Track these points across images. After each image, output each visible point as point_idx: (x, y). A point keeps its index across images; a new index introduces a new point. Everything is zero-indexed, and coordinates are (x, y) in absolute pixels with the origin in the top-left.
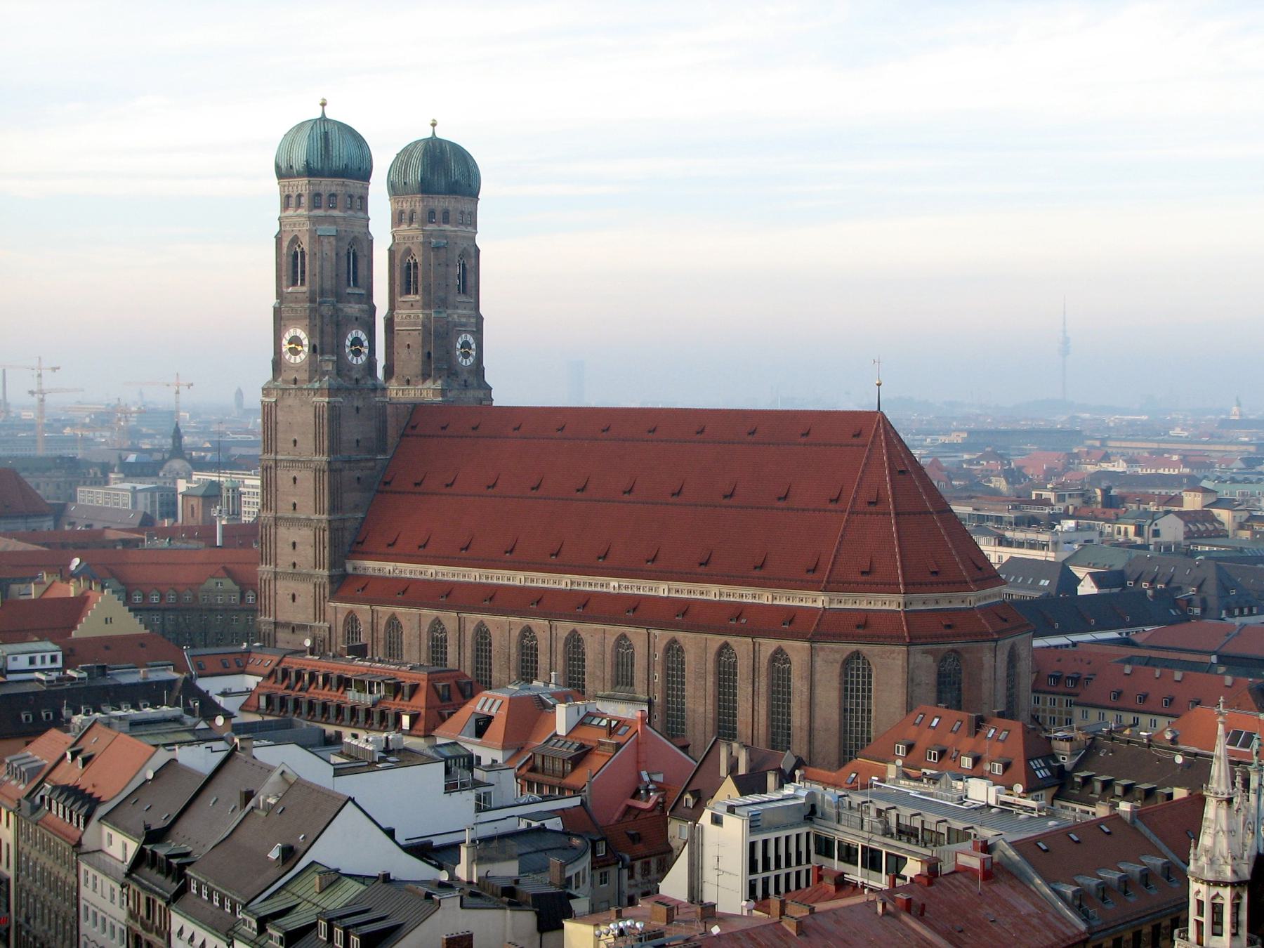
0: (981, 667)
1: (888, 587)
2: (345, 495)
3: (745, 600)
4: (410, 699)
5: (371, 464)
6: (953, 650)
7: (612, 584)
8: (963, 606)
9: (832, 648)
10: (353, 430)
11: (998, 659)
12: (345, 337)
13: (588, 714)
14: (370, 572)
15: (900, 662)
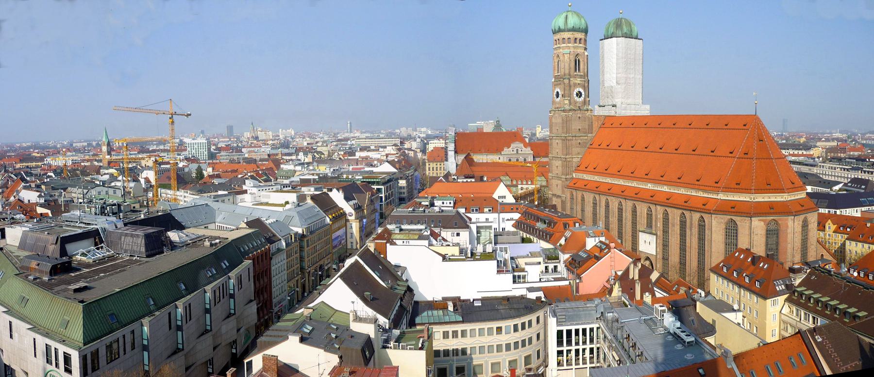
0: (787, 227)
1: (747, 191)
2: (573, 149)
3: (693, 194)
4: (553, 227)
5: (587, 138)
6: (774, 220)
7: (649, 185)
8: (782, 200)
9: (720, 217)
10: (576, 125)
11: (796, 224)
12: (574, 91)
13: (601, 242)
14: (580, 177)
15: (748, 225)
